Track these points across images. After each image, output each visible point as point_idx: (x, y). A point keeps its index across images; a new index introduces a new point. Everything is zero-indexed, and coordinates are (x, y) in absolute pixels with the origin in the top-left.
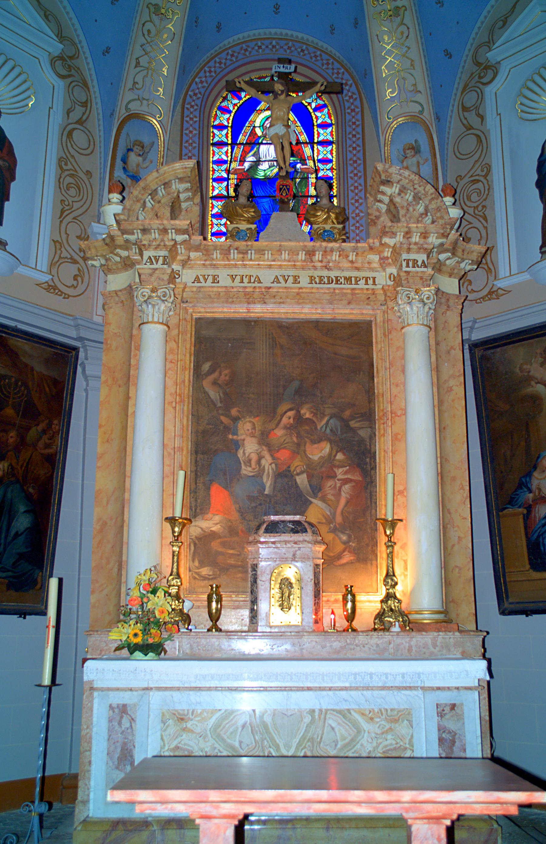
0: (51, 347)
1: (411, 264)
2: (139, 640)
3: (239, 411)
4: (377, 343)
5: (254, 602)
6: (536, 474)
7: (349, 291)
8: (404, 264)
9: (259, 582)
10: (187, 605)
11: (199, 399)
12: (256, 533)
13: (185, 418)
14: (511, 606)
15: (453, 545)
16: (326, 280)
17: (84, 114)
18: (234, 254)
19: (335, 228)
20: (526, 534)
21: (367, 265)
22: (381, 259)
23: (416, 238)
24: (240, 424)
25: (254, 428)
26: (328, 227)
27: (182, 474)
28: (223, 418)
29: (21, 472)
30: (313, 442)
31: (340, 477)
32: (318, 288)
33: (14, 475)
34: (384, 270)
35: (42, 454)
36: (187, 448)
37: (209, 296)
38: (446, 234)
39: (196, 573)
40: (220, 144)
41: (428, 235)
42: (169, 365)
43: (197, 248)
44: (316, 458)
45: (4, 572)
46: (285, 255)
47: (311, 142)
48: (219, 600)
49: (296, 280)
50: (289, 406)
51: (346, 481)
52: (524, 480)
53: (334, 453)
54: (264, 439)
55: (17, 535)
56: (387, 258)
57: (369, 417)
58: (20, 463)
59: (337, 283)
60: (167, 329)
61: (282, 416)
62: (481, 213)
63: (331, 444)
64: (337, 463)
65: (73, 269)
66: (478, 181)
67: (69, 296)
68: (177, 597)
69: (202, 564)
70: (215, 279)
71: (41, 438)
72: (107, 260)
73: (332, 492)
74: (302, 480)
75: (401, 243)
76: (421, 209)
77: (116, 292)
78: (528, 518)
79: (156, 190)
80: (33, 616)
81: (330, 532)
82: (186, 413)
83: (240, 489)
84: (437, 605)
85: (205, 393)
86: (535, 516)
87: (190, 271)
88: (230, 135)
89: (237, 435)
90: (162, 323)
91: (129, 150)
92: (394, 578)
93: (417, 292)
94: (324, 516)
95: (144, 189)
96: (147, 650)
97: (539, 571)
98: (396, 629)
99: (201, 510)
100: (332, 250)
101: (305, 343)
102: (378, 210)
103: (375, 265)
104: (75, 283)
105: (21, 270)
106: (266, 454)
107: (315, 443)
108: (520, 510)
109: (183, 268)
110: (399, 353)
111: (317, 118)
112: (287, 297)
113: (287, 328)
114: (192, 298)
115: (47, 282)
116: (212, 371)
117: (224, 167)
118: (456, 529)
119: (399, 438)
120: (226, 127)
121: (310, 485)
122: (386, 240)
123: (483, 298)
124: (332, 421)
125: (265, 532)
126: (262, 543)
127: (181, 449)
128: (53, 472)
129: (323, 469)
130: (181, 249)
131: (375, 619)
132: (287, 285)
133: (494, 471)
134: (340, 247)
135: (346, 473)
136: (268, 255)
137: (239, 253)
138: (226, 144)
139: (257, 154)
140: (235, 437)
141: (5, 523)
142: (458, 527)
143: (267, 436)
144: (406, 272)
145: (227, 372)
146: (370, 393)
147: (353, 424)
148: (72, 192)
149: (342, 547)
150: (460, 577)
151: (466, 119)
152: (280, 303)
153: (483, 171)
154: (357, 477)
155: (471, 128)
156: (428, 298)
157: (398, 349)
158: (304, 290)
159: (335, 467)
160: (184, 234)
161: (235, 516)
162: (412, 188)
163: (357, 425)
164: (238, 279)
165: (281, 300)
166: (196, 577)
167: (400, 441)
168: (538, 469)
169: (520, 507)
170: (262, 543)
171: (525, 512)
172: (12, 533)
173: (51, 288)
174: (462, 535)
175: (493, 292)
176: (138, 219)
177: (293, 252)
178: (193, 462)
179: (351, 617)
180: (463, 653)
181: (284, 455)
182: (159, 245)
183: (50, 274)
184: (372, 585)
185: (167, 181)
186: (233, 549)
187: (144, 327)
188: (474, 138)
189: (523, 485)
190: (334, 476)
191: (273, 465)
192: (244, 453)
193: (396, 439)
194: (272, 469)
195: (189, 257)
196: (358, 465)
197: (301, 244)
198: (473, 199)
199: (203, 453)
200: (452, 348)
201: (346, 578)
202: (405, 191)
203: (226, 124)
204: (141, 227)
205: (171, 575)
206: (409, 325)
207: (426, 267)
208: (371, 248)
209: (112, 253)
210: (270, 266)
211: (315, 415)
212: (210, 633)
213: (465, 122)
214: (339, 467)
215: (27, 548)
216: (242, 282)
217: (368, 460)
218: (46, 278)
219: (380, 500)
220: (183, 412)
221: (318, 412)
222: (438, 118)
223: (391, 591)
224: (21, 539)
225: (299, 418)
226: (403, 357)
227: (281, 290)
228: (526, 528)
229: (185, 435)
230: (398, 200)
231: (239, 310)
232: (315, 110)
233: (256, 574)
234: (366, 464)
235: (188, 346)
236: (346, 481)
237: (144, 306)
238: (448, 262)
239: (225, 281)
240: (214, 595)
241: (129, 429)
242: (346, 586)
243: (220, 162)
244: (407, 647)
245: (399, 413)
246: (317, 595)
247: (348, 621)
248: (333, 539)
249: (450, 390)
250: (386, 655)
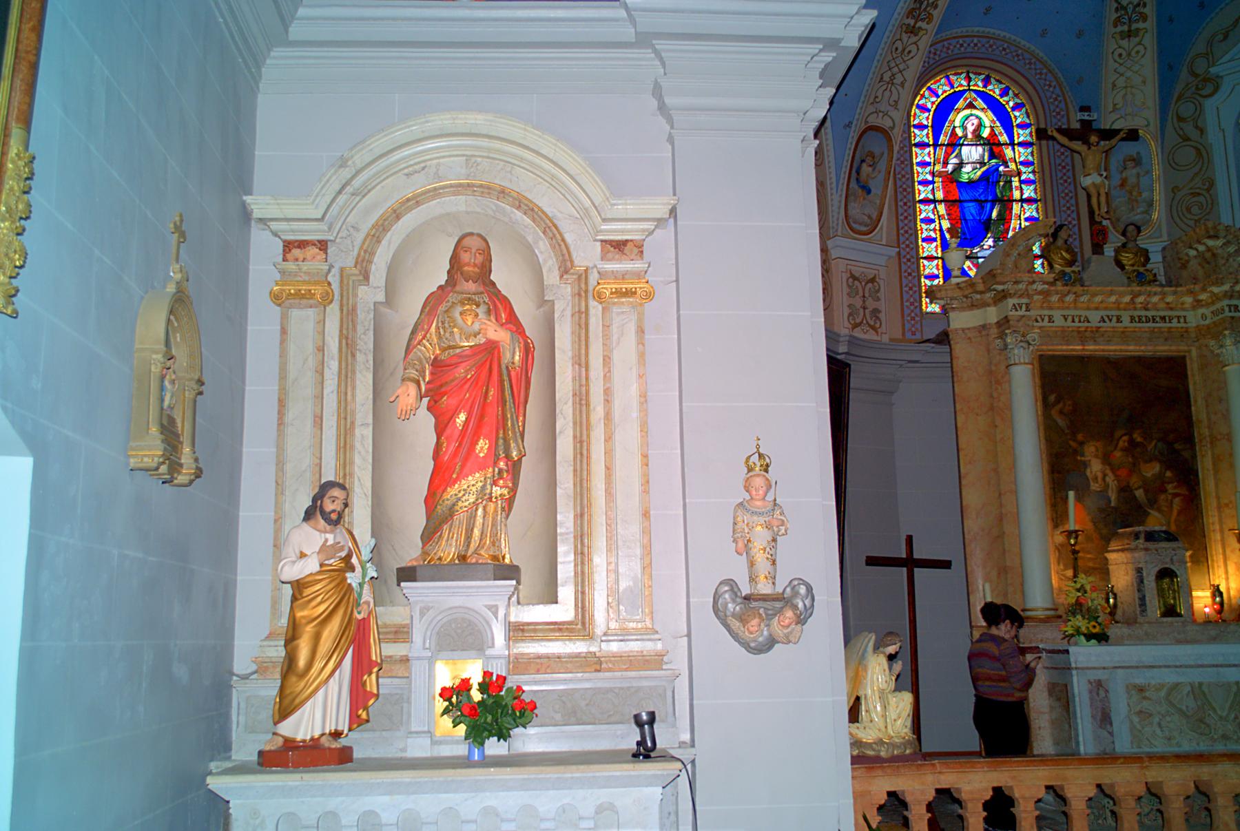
28: (1072, 443)
30: (1146, 462)
40: (922, 145)
44: (1149, 475)
47: (1012, 144)
51: (1176, 495)
54: (1106, 459)
74: (1139, 494)
85: (1055, 421)
91: (863, 161)
106: (1108, 471)
116: (1057, 401)
117: (928, 169)
120: (926, 127)
135: (1175, 488)
138: (928, 145)
139: (959, 156)
147: (1177, 446)
154: (1183, 491)
155: (1189, 139)
164: (1070, 319)
181: (1123, 473)
188: (1193, 152)
190: (1164, 490)
210: (1097, 309)
225: (1132, 442)
232: (1013, 109)
236: (1176, 495)
243: (924, 164)
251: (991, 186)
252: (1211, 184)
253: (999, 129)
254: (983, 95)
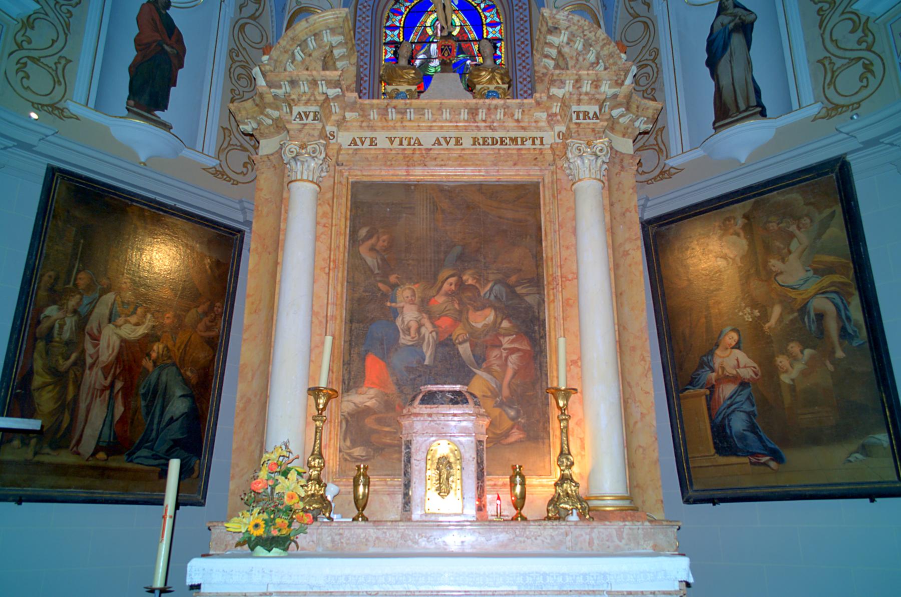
0: (214, 228)
1: (581, 116)
2: (260, 532)
3: (397, 278)
4: (544, 204)
5: (407, 486)
6: (718, 352)
7: (515, 152)
8: (574, 116)
9: (413, 461)
10: (331, 492)
11: (355, 266)
12: (411, 405)
13: (340, 285)
14: (695, 493)
15: (636, 423)
16: (490, 141)
17: (257, 10)
18: (392, 115)
19: (500, 88)
20: (710, 416)
21: (534, 124)
22: (549, 116)
23: (586, 87)
24: (399, 291)
25: (414, 295)
26: (492, 87)
27: (329, 340)
28: (381, 285)
29: (178, 354)
30: (477, 309)
31: (506, 346)
32: (481, 149)
33: (170, 358)
34: (552, 129)
35: (202, 337)
36: (341, 316)
37: (367, 159)
38: (620, 81)
39: (347, 454)
41: (599, 83)
42: (321, 229)
43: (352, 107)
44: (479, 325)
45: (156, 459)
46: (446, 115)
48: (367, 484)
49: (458, 142)
50: (451, 272)
51: (512, 351)
52: (705, 359)
53: (499, 320)
54: (424, 306)
55: (172, 420)
56: (555, 115)
57: (537, 282)
58: (177, 345)
59: (501, 144)
60: (318, 189)
61: (443, 283)
62: (650, 96)
63: (495, 311)
64: (503, 332)
65: (243, 157)
66: (646, 65)
67: (238, 183)
68: (319, 481)
69: (354, 444)
70: (373, 142)
71: (201, 320)
72: (259, 124)
73: (497, 362)
74: (465, 350)
75: (571, 94)
76: (592, 57)
77: (268, 156)
78: (711, 398)
79: (305, 41)
80: (189, 507)
81: (497, 406)
82: (340, 280)
83: (399, 360)
84: (621, 490)
85: (362, 259)
86: (719, 396)
87: (346, 134)
88: (401, 35)
89: (395, 302)
90: (312, 182)
92: (570, 457)
93: (589, 144)
94: (489, 390)
95: (293, 39)
96: (271, 544)
97: (727, 456)
98: (574, 518)
99: (355, 383)
100: (496, 108)
101: (468, 207)
102: (545, 67)
103: (543, 124)
104: (245, 170)
105: (187, 153)
107: (478, 310)
108: (702, 390)
109: (339, 130)
110: (570, 214)
111: (486, 17)
112: (449, 159)
113: (448, 191)
114: (347, 161)
115: (214, 167)
116: (369, 236)
118: (638, 404)
119: (572, 303)
121: (474, 355)
122: (554, 91)
123: (655, 179)
124: (496, 287)
125: (420, 404)
126: (416, 415)
127: (334, 317)
128: (215, 356)
129: (488, 338)
130: (335, 107)
131: (549, 505)
132: (449, 146)
133: (672, 350)
134: (505, 104)
135: (512, 342)
136: (428, 115)
137: (398, 112)
139: (428, 52)
140: (393, 304)
141: (158, 408)
142: (640, 401)
143: (428, 303)
144: (576, 123)
145: (385, 237)
146: (538, 258)
147: (519, 290)
148: (243, 82)
149: (511, 423)
150: (644, 458)
151: (632, 8)
152: (441, 166)
153: (650, 55)
154: (525, 346)
156: (601, 151)
157: (568, 210)
158: (467, 152)
159: (501, 335)
160: (335, 87)
161: (392, 389)
162: (581, 35)
163: (524, 291)
164: (397, 141)
165: (443, 163)
166: (346, 458)
167: (571, 306)
168: (720, 347)
169: (702, 388)
170: (416, 415)
171: (708, 392)
172: (167, 418)
173: (218, 173)
174: (645, 411)
175: (665, 172)
176: (285, 70)
177: (455, 111)
178: (348, 331)
179: (519, 503)
180: (655, 547)
181: (444, 323)
182: (309, 100)
183: (218, 159)
184: (544, 467)
185: (317, 31)
186: (389, 426)
187: (293, 184)
188: (641, 25)
189: (705, 364)
190: (500, 345)
191: (434, 334)
192: (403, 322)
193: (568, 305)
194: (433, 337)
195: (344, 117)
196: (526, 333)
197: (463, 101)
198: (641, 83)
199: (359, 322)
200: (627, 210)
201: (514, 458)
202: (574, 39)
203: (398, 24)
204: (289, 79)
205: (312, 454)
206: (580, 180)
207: (597, 118)
208: (538, 104)
209: (262, 113)
210: (430, 128)
211: (478, 281)
212: (355, 522)
213: (631, 11)
214: (505, 335)
215: (182, 434)
216: (401, 144)
217: (536, 328)
218: (215, 163)
219: (551, 372)
220: (337, 279)
221: (481, 278)
222: (604, 6)
223: (566, 472)
224: (176, 425)
225: (461, 285)
226: (574, 218)
227: (442, 152)
228: (709, 409)
229: (339, 302)
230: (566, 50)
231: (398, 174)
232: (484, 10)
233: (409, 453)
234: (534, 332)
235: (343, 211)
236: (512, 351)
237: (293, 163)
238: (621, 120)
239: (383, 142)
240: (361, 477)
241: (276, 297)
242: (514, 468)
244: (587, 540)
245: (570, 277)
246: (480, 477)
247: (516, 509)
248: (500, 415)
249: (626, 254)
250: (563, 549)
252: (657, 52)
253: (469, 27)
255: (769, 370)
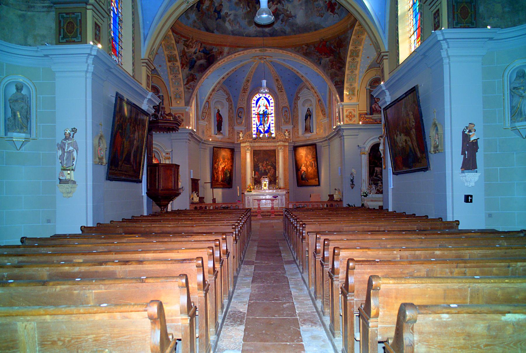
54: (262, 166)
57: (275, 163)
146: (276, 159)
173: (229, 138)
251: (265, 114)
254: (265, 97)
255: (307, 170)
